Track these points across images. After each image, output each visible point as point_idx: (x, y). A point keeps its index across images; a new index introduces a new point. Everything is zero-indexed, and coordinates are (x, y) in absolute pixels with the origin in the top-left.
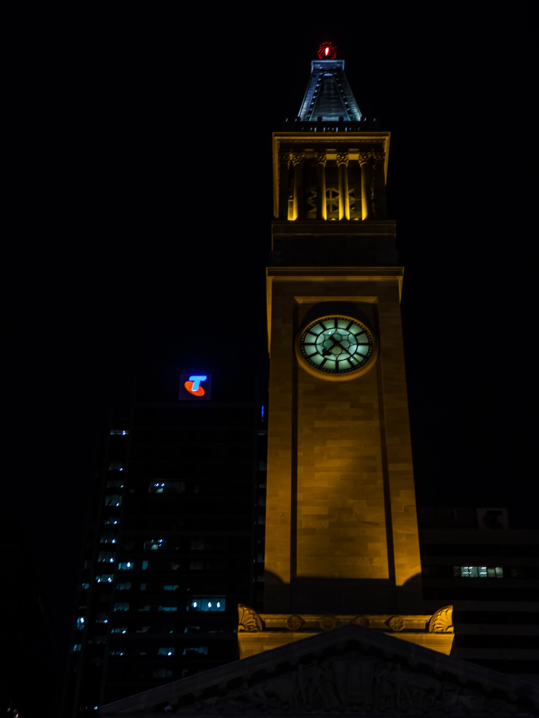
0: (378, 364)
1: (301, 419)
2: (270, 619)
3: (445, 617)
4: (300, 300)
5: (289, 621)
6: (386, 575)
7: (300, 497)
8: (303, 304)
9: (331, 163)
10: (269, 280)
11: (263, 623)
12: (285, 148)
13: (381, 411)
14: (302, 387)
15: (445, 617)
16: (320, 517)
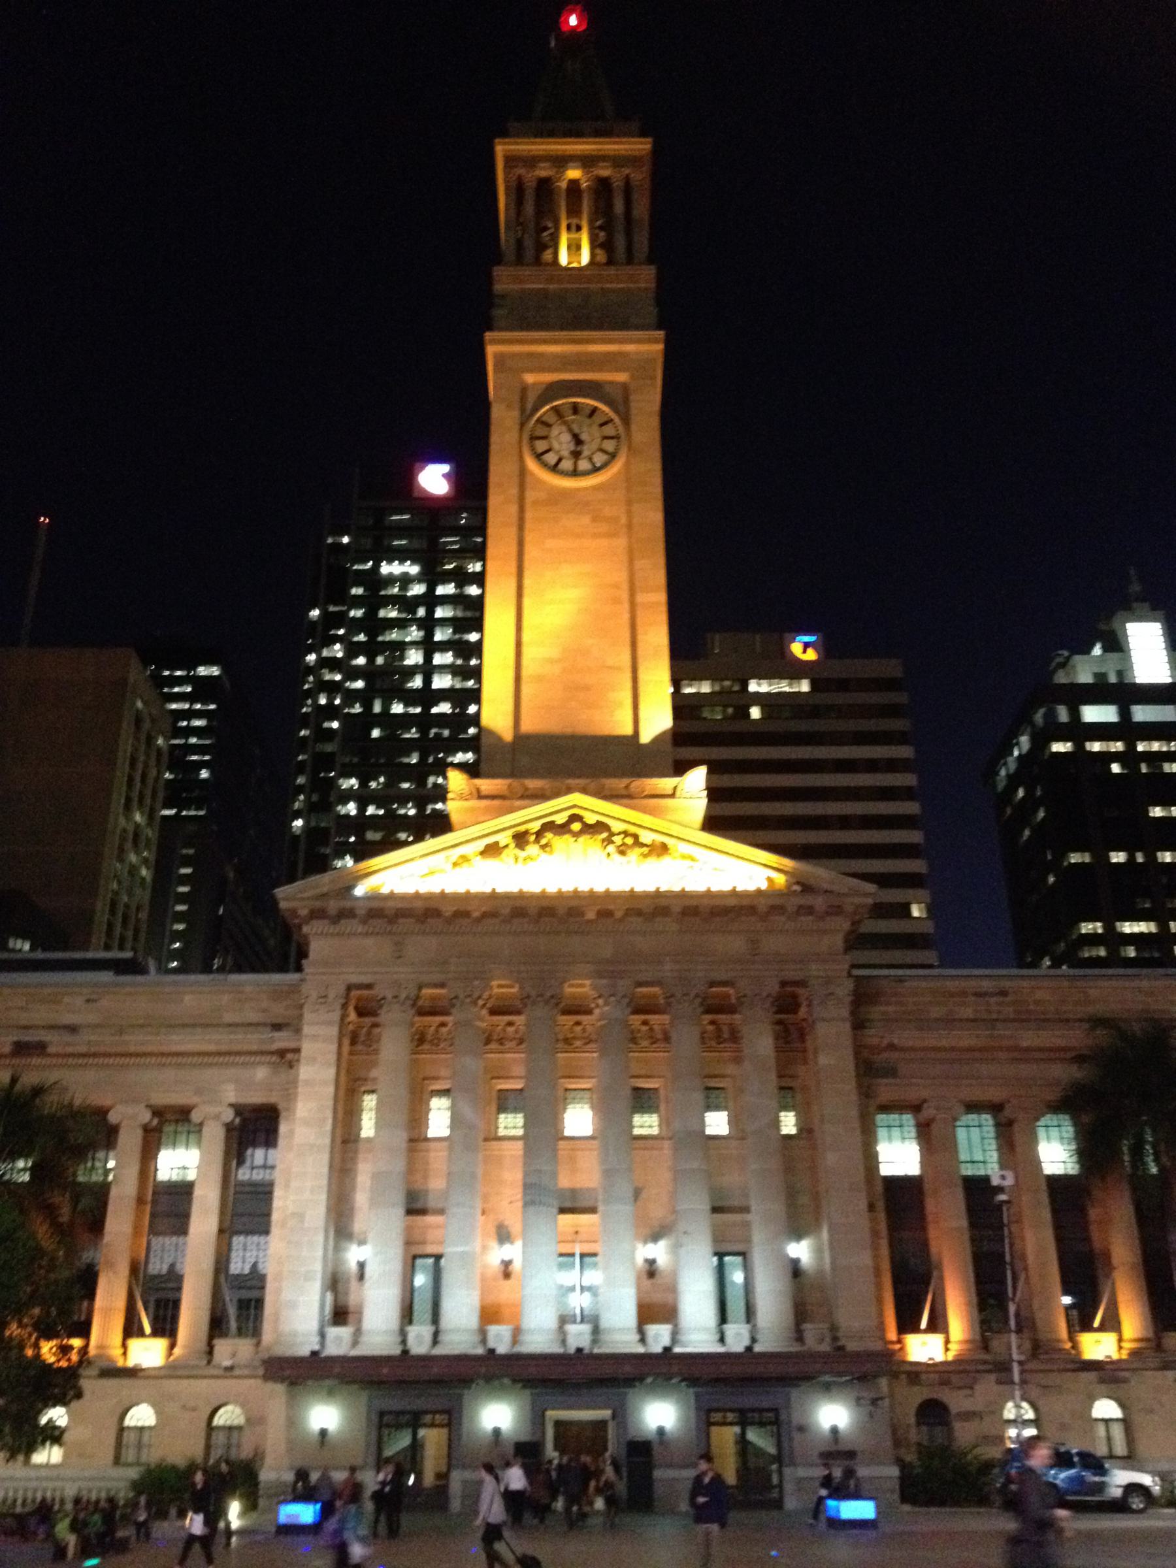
0: (627, 464)
1: (529, 538)
2: (486, 785)
3: (697, 777)
4: (530, 378)
5: (510, 786)
6: (628, 730)
7: (526, 637)
8: (534, 384)
9: (574, 183)
10: (491, 350)
11: (478, 790)
12: (511, 161)
13: (630, 526)
14: (530, 495)
15: (697, 777)
16: (551, 661)
